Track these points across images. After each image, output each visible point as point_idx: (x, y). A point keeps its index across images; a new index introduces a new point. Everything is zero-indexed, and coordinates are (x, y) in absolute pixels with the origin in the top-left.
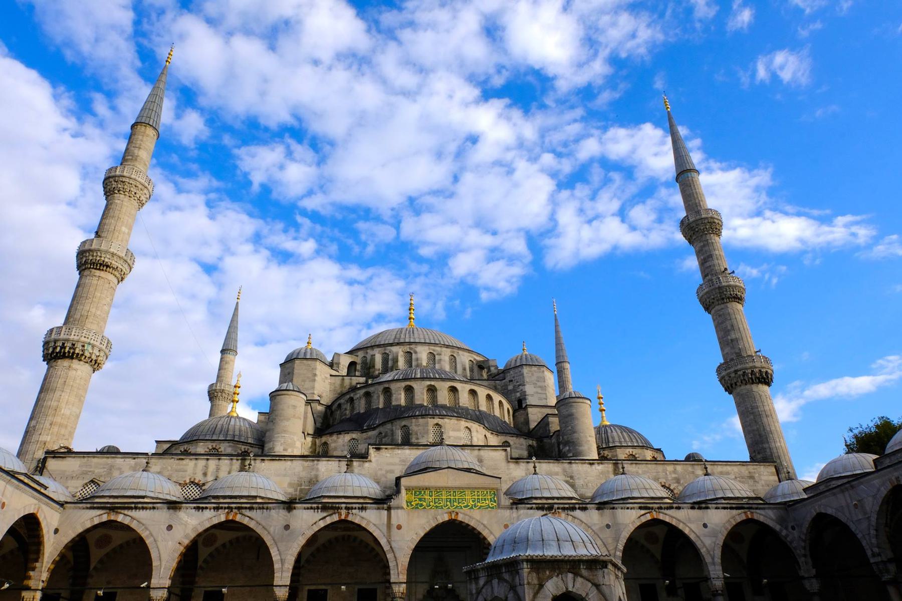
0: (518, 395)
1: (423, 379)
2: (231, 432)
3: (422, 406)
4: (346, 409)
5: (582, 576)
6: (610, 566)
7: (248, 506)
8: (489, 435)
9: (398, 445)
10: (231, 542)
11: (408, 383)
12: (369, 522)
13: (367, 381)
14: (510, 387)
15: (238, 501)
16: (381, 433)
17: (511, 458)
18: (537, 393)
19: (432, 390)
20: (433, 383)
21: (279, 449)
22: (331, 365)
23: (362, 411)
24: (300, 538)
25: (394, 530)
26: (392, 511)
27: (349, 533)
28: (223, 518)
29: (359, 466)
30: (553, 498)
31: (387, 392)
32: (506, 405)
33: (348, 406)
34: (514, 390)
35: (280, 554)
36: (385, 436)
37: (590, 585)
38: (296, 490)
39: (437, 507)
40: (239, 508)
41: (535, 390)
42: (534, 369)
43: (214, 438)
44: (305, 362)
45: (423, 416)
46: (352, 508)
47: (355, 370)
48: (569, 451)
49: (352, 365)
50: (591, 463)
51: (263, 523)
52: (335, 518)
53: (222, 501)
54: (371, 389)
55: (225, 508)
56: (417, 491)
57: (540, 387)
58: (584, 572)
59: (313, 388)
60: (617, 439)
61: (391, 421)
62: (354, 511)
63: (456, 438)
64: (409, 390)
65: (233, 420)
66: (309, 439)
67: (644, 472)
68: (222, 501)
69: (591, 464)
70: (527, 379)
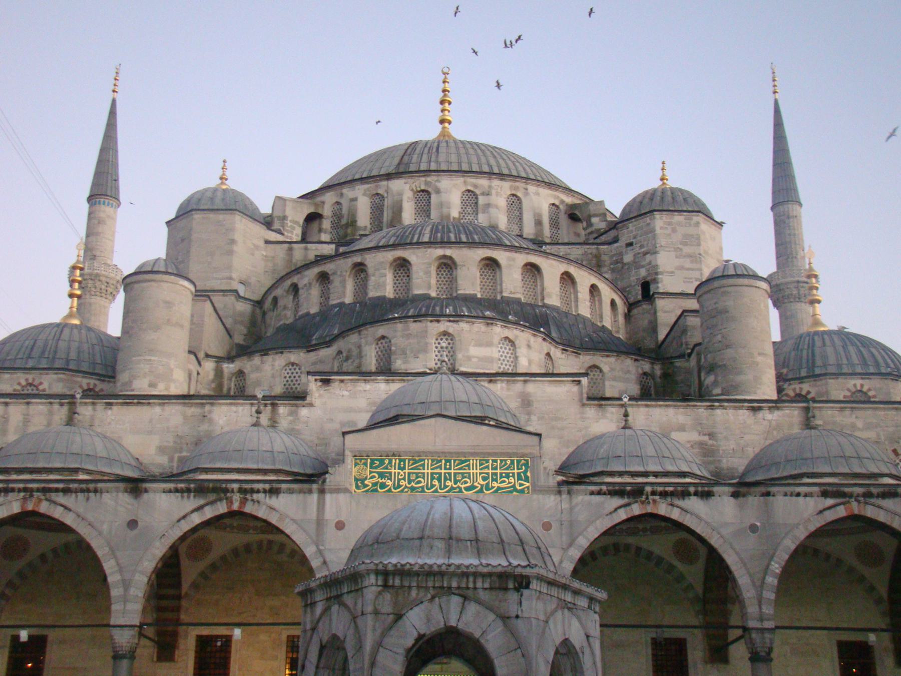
0: (643, 272)
1: (431, 244)
2: (61, 354)
3: (426, 297)
4: (285, 308)
5: (479, 602)
6: (534, 585)
7: (61, 486)
8: (556, 353)
9: (370, 374)
10: (54, 551)
11: (399, 253)
12: (283, 516)
13: (337, 250)
14: (628, 258)
15: (44, 477)
16: (340, 352)
17: (589, 398)
18: (682, 268)
19: (447, 265)
20: (448, 252)
21: (141, 386)
22: (268, 222)
23: (314, 310)
24: (158, 544)
25: (330, 530)
26: (328, 497)
27: (270, 537)
28: (16, 508)
29: (290, 414)
30: (645, 474)
31: (360, 269)
32: (607, 293)
33: (288, 301)
34: (636, 264)
35: (121, 570)
36: (347, 358)
37: (492, 616)
38: (171, 459)
39: (413, 489)
40: (45, 490)
41: (678, 262)
42: (678, 218)
43: (30, 364)
44: (211, 216)
45: (417, 317)
46: (252, 491)
47: (320, 230)
48: (715, 383)
49: (313, 218)
50: (755, 406)
51: (90, 516)
52: (222, 508)
53: (14, 477)
54: (329, 267)
55: (20, 490)
56: (377, 459)
57: (690, 256)
58: (483, 595)
59: (229, 267)
60: (832, 360)
61: (358, 327)
62: (255, 496)
63: (481, 359)
64: (402, 265)
65: (67, 331)
66: (209, 366)
67: (868, 427)
68: (14, 477)
69: (755, 410)
70: (663, 243)
